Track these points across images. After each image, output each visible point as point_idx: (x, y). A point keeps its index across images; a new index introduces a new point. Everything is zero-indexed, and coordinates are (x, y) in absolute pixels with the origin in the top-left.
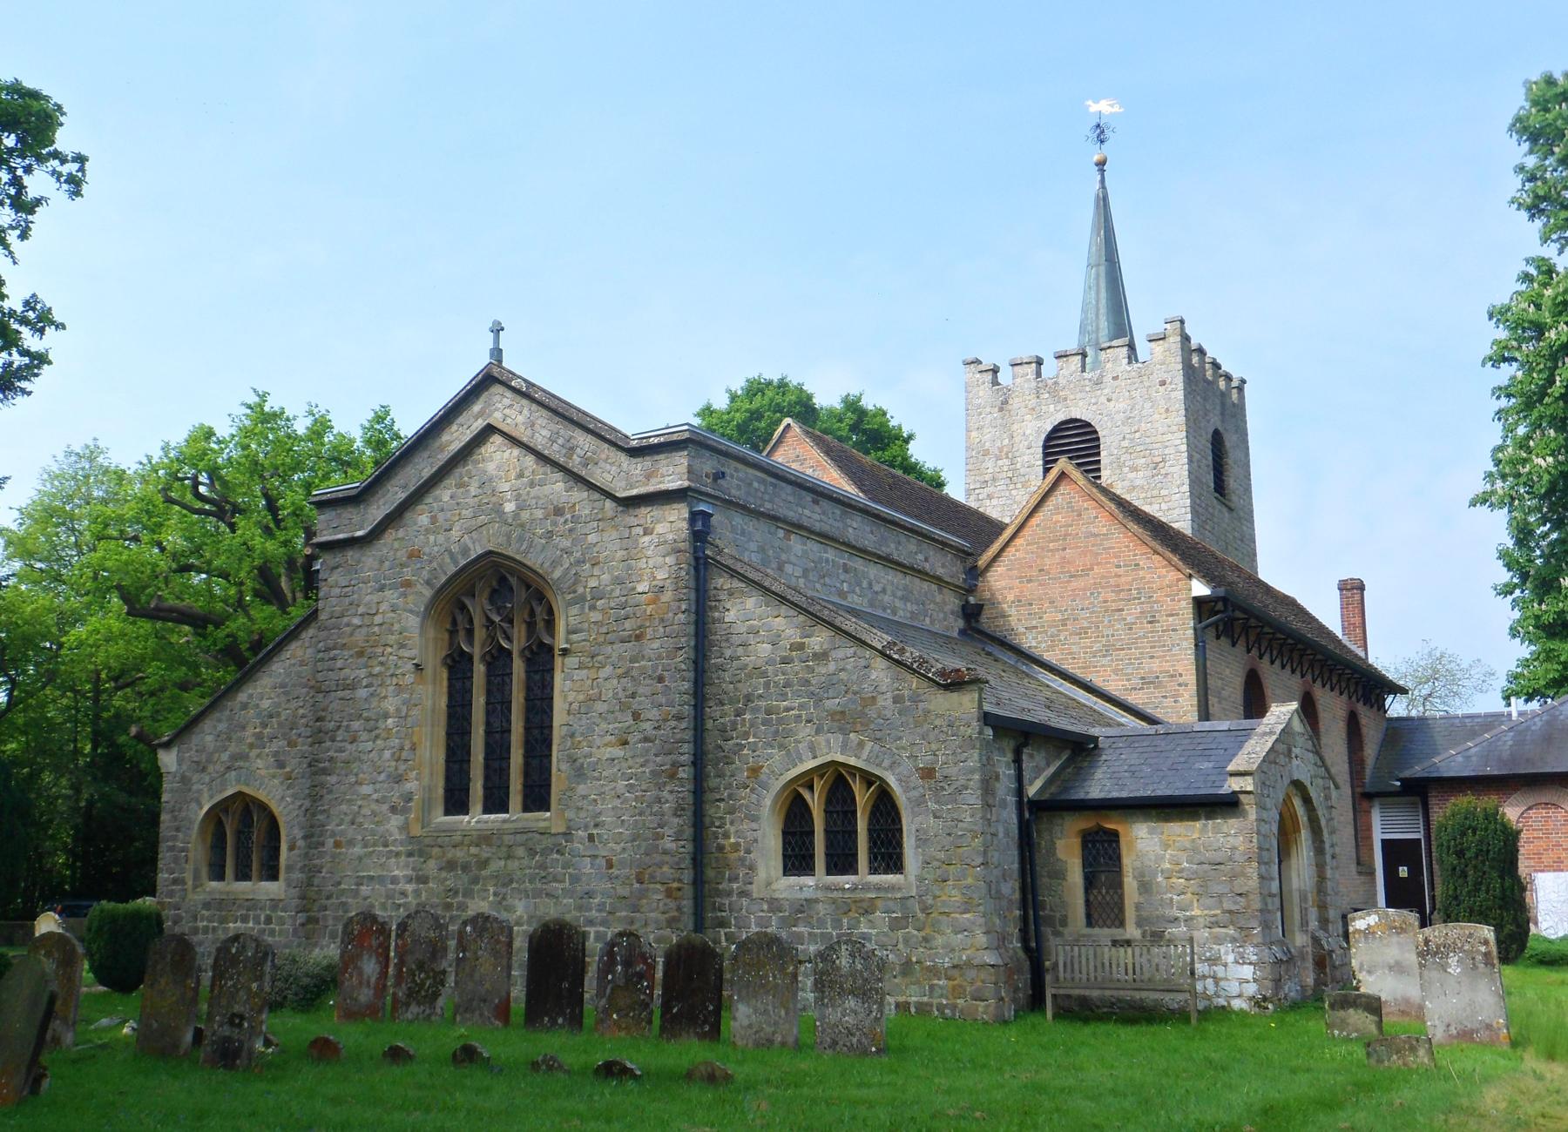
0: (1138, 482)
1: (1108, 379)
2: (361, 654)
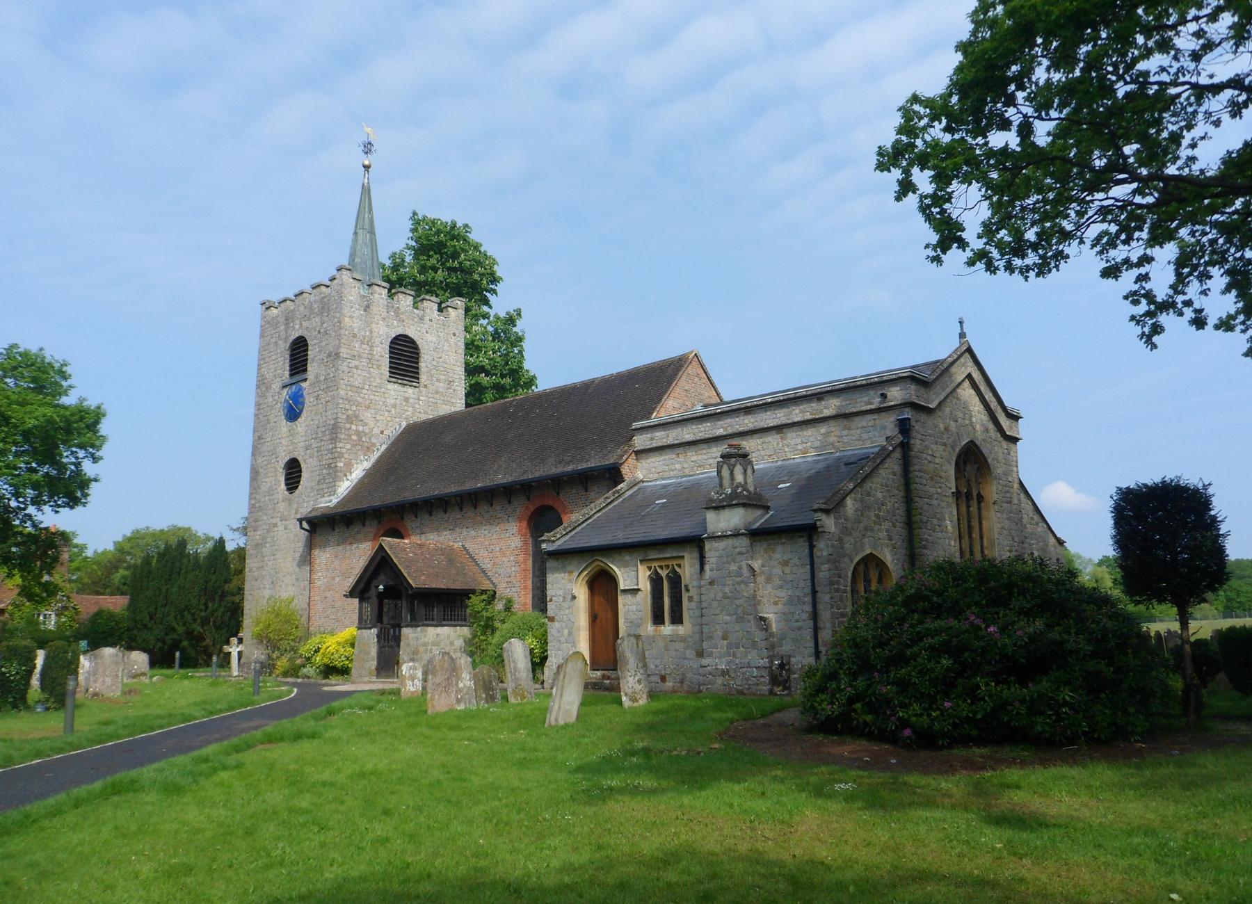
1: (427, 318)
2: (931, 479)
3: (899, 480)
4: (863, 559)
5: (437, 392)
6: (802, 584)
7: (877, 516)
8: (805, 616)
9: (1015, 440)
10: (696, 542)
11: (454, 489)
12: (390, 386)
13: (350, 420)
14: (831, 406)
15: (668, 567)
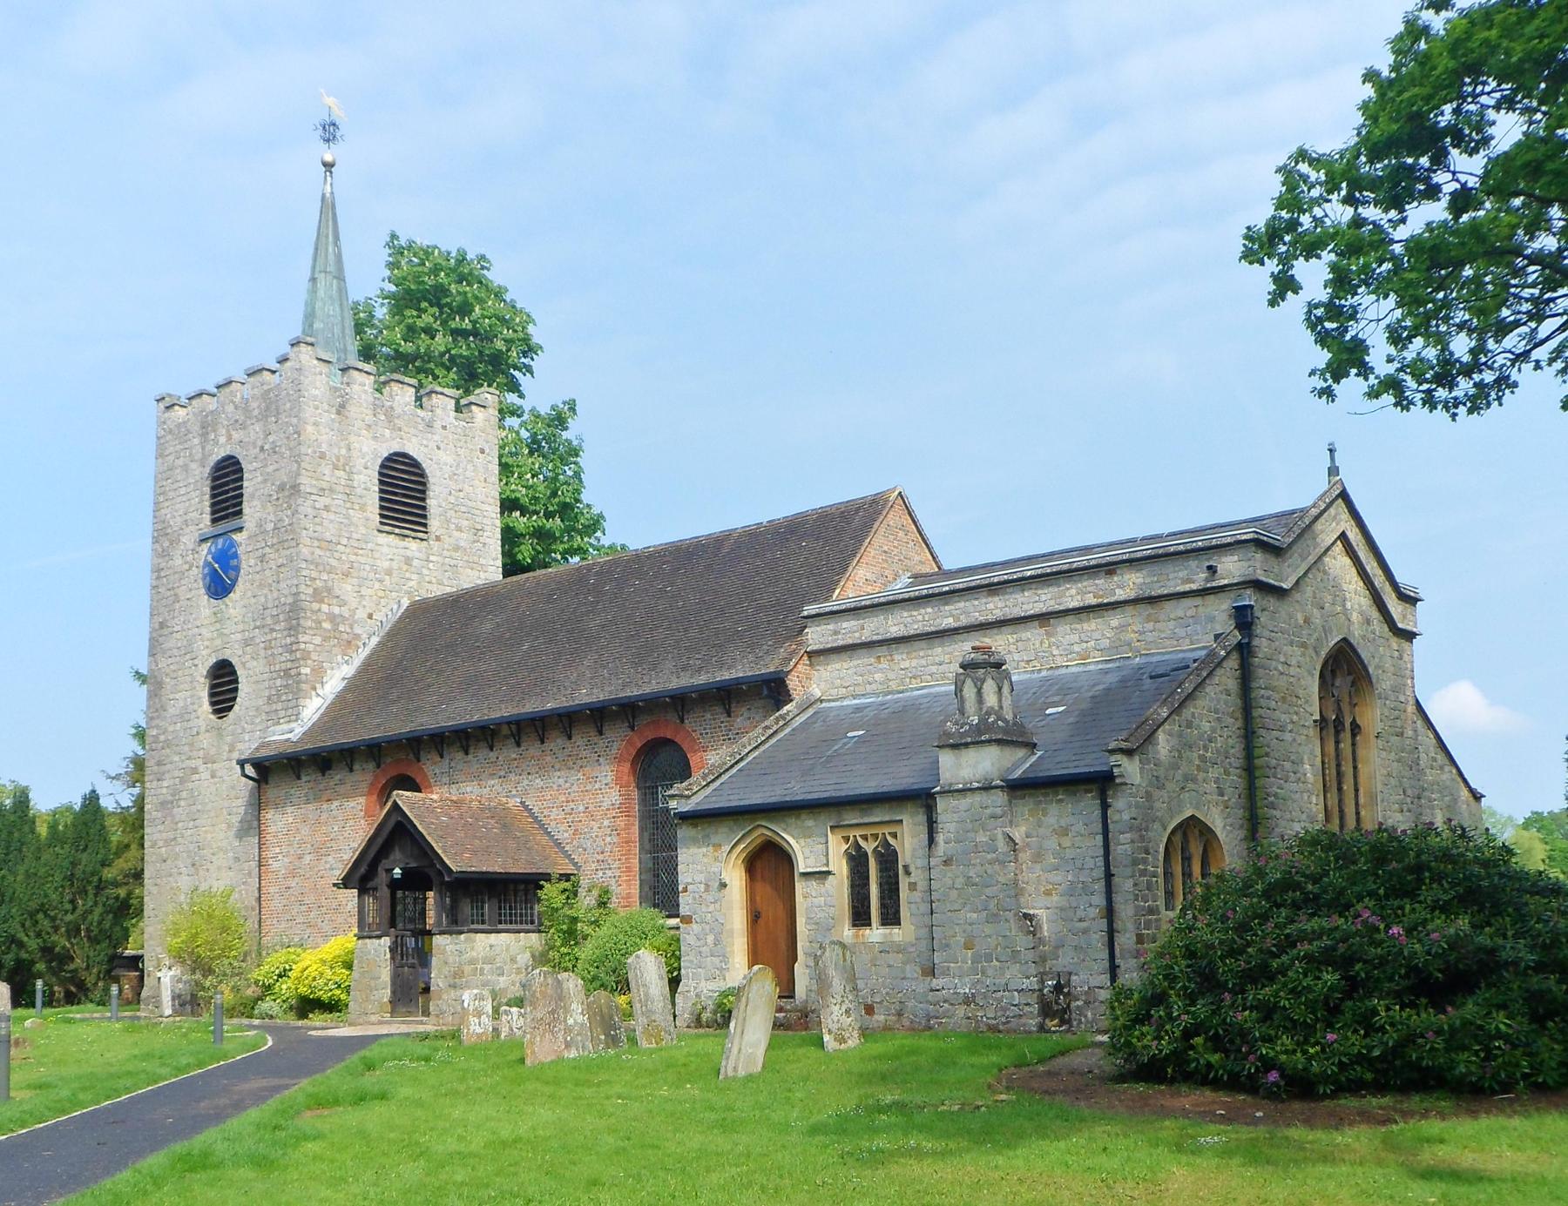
0: (462, 544)
1: (438, 425)
2: (1284, 699)
3: (1234, 702)
4: (1180, 825)
5: (457, 548)
6: (1090, 863)
7: (1203, 758)
8: (1094, 912)
9: (1410, 636)
10: (923, 799)
11: (506, 711)
12: (383, 539)
13: (318, 596)
14: (1128, 584)
15: (876, 836)
